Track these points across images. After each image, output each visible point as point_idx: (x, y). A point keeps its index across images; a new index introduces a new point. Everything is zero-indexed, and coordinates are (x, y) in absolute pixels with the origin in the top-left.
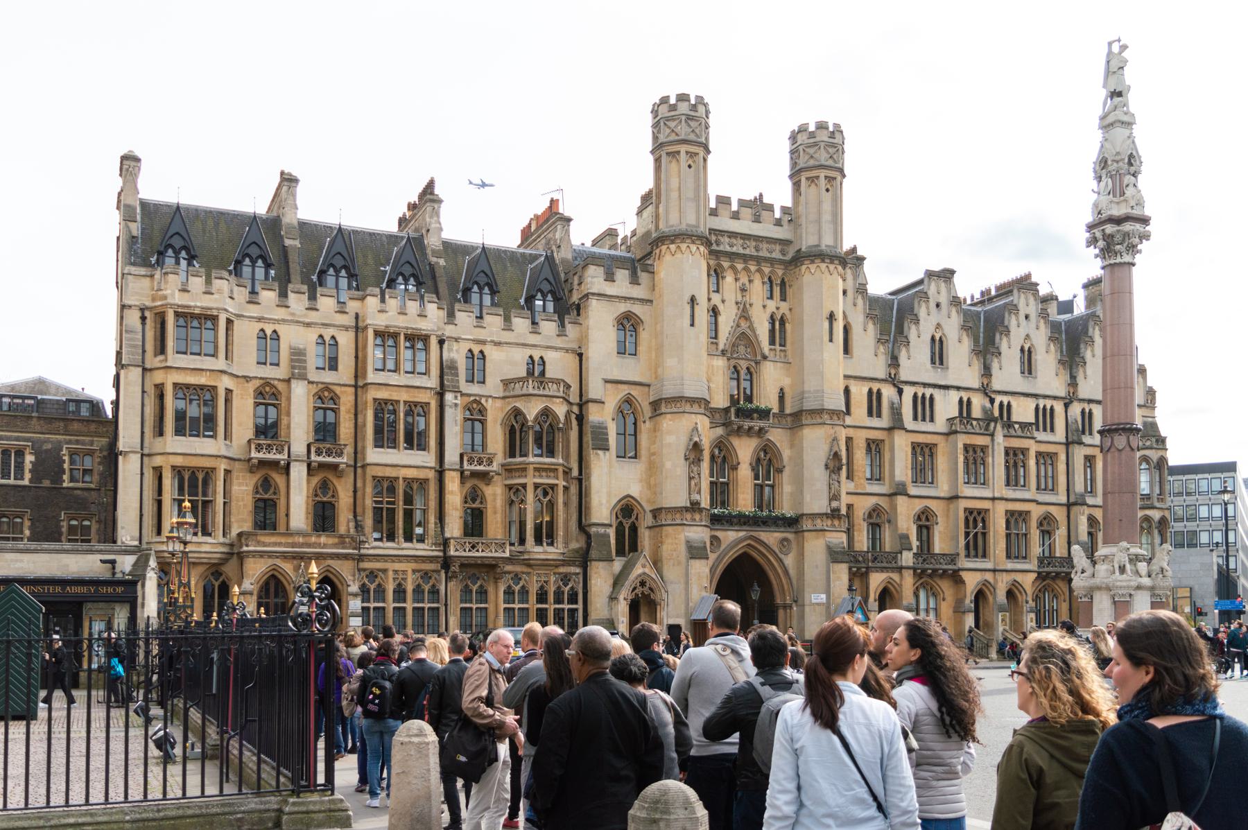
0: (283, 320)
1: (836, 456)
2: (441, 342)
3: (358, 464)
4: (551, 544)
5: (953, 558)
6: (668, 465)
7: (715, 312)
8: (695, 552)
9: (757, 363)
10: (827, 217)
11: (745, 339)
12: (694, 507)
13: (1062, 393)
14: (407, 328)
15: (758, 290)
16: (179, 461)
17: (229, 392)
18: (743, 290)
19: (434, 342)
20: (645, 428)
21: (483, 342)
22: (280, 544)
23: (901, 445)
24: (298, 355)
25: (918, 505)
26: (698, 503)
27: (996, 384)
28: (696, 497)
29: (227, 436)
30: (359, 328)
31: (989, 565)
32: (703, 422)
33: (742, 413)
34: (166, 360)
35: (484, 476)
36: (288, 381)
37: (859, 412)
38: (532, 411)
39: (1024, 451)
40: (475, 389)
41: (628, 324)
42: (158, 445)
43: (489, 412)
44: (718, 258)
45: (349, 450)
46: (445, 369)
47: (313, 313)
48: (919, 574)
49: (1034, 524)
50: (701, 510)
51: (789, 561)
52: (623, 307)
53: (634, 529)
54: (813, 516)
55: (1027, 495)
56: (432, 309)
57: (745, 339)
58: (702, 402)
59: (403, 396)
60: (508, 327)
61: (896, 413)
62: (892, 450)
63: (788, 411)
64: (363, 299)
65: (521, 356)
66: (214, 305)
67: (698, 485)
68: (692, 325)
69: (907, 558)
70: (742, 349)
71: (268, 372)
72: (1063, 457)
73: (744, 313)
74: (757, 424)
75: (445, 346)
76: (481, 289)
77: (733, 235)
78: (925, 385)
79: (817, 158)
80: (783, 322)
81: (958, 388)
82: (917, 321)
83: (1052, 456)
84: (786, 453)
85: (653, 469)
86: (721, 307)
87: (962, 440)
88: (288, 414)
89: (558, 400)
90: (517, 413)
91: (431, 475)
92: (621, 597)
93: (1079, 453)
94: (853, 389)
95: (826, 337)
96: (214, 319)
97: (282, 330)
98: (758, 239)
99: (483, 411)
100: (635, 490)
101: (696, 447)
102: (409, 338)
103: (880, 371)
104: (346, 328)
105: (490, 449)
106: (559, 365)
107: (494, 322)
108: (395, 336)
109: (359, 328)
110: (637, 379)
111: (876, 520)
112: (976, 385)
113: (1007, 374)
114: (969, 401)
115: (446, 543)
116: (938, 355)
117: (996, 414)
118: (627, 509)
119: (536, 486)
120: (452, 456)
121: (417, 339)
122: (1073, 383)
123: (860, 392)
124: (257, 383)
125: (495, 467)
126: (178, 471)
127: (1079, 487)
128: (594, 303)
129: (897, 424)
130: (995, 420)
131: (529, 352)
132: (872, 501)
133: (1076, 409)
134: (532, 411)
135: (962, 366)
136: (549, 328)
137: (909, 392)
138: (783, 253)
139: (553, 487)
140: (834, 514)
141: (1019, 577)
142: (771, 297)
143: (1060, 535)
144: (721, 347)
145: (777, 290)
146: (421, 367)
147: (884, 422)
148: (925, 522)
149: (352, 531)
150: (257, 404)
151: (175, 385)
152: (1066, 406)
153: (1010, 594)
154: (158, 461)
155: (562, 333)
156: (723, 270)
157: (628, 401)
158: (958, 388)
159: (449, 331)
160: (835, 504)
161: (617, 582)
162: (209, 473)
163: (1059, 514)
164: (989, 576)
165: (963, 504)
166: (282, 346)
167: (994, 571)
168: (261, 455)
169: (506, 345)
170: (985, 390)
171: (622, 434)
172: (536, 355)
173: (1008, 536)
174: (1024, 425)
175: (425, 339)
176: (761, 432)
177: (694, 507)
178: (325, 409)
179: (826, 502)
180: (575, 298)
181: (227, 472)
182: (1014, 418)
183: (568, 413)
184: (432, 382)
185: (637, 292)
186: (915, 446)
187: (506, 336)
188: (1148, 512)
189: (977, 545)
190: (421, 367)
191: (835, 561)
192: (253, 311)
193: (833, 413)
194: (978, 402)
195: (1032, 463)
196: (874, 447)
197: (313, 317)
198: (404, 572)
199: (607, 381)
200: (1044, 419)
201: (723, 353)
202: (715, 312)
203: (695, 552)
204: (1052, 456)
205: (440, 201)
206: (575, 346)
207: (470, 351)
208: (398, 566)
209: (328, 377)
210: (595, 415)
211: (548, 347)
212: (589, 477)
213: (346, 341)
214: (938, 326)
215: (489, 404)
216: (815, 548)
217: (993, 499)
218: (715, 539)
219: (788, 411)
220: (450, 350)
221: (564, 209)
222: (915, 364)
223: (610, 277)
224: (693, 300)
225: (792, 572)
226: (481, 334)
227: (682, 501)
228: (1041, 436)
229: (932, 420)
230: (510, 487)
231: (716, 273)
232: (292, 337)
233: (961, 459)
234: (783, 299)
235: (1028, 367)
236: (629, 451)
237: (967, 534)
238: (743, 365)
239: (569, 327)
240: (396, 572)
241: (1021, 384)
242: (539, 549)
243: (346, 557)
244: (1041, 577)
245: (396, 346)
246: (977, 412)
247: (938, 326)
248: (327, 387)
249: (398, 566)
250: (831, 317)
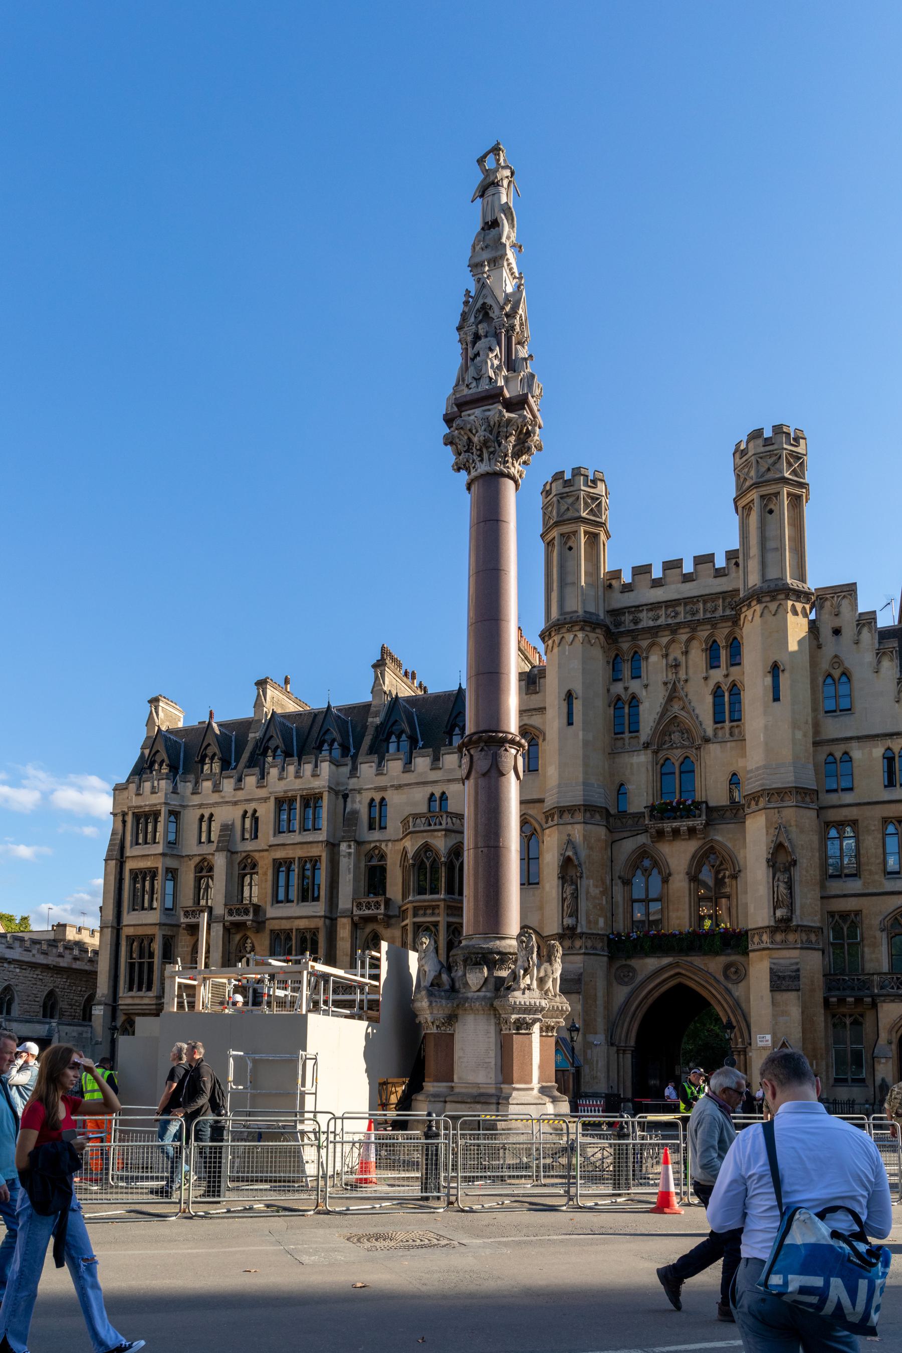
0: (216, 803)
9: (698, 748)
14: (302, 789)
21: (384, 789)
40: (376, 835)
43: (389, 856)
44: (634, 639)
59: (298, 853)
68: (570, 723)
70: (676, 737)
73: (673, 694)
74: (683, 825)
75: (349, 800)
86: (642, 694)
89: (440, 834)
97: (216, 811)
99: (383, 857)
159: (353, 783)
187: (409, 778)
192: (196, 800)
197: (240, 795)
201: (647, 746)
211: (449, 781)
220: (353, 802)
226: (382, 781)
232: (227, 815)
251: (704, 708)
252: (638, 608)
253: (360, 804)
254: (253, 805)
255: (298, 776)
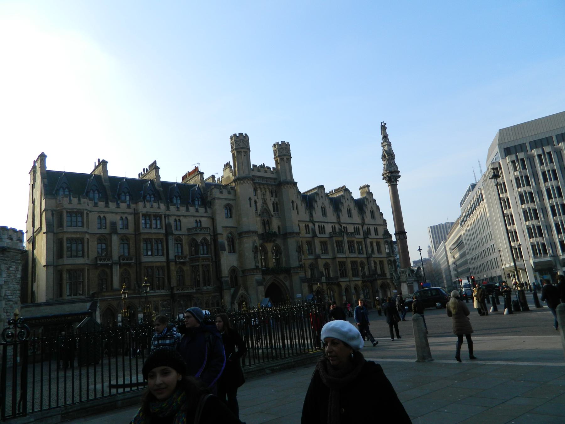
1: (299, 247)
2: (165, 217)
3: (139, 263)
4: (209, 285)
5: (336, 278)
6: (247, 254)
7: (256, 202)
8: (259, 283)
9: (270, 218)
10: (288, 170)
11: (265, 210)
12: (257, 267)
13: (360, 222)
15: (268, 194)
16: (69, 267)
17: (88, 239)
18: (264, 194)
19: (163, 216)
20: (237, 242)
21: (179, 216)
22: (111, 296)
23: (317, 241)
24: (114, 225)
25: (324, 262)
26: (258, 266)
27: (342, 221)
28: (257, 264)
29: (88, 257)
30: (136, 214)
31: (348, 279)
32: (256, 239)
33: (267, 236)
34: (63, 229)
35: (184, 263)
36: (110, 234)
37: (303, 231)
38: (199, 239)
39: (353, 242)
41: (229, 208)
42: (60, 262)
45: (134, 258)
46: (168, 226)
47: (118, 209)
48: (328, 284)
49: (359, 264)
50: (259, 269)
51: (287, 283)
52: (226, 202)
53: (236, 278)
54: (294, 268)
55: (355, 256)
56: (162, 206)
57: (265, 210)
58: (255, 232)
60: (188, 210)
61: (314, 231)
62: (314, 244)
63: (281, 233)
64: (136, 203)
65: (193, 220)
66: (81, 208)
67: (258, 260)
68: (251, 206)
69: (324, 279)
71: (102, 231)
72: (363, 243)
73: (265, 202)
76: (176, 198)
77: (259, 177)
78: (322, 222)
79: (283, 152)
80: (277, 204)
81: (331, 223)
82: (316, 201)
83: (361, 242)
84: (282, 248)
85: (241, 257)
86: (257, 200)
87: (335, 239)
88: (111, 246)
90: (194, 240)
91: (165, 264)
92: (235, 302)
93: (368, 241)
94: (300, 225)
95: (292, 209)
96: (82, 214)
97: (107, 216)
98: (266, 178)
99: (181, 240)
100: (235, 264)
101: (256, 247)
102: (154, 216)
103: (308, 220)
104: (131, 214)
105: (185, 253)
106: (206, 222)
107: (183, 209)
108: (150, 216)
109: (136, 214)
110: (233, 226)
111: (313, 267)
112: (336, 221)
113: (344, 218)
114: (335, 227)
115: (172, 289)
116: (324, 213)
117: (343, 230)
118: (233, 270)
119: (203, 265)
120: (172, 256)
121: (157, 216)
122: (363, 219)
123: (302, 225)
124: (98, 235)
125: (187, 259)
126: (69, 271)
127: (370, 252)
128: (217, 201)
129: (315, 235)
130: (344, 232)
131: (195, 218)
132: (310, 261)
133: (365, 227)
134: (199, 239)
135: (331, 216)
136: (202, 210)
137: (317, 225)
138: (275, 182)
139: (208, 265)
140: (301, 267)
141: (356, 282)
142: (272, 196)
143: (366, 267)
144: (259, 213)
145: (274, 194)
146: (159, 226)
147: (310, 235)
148: (326, 266)
149: (137, 288)
150: (98, 243)
151: (67, 238)
152: (362, 226)
153: (355, 288)
154: (60, 268)
155: (206, 211)
156: (257, 188)
157: (231, 233)
158: (331, 223)
159: (168, 213)
160: (301, 263)
161: (233, 297)
162: (82, 270)
163: (365, 261)
164: (348, 283)
165: (338, 260)
166: (107, 221)
167: (349, 281)
168: (101, 262)
169: (188, 218)
170: (339, 222)
171: (229, 245)
172: (198, 219)
173: (352, 269)
174: (351, 233)
175: (160, 216)
176: (274, 241)
177: (257, 267)
178: (124, 243)
179: (298, 263)
180: (209, 199)
181: (88, 269)
182: (348, 231)
183: (211, 239)
184: (163, 231)
185: (230, 197)
186: (321, 242)
187: (187, 214)
188: (390, 258)
189: (344, 274)
190: (159, 226)
191: (304, 282)
192: (96, 209)
193: (298, 233)
194: (337, 227)
195: (356, 245)
196: (309, 243)
198: (158, 301)
199: (223, 227)
200: (357, 230)
201: (259, 215)
202: (256, 202)
203: (259, 283)
204: (361, 242)
205: (159, 168)
206: (210, 216)
207: (175, 219)
208: (155, 299)
209: (125, 231)
210: (220, 240)
212: (219, 261)
213: (131, 218)
214: (323, 203)
215: (183, 238)
216: (296, 279)
217: (346, 258)
218: (264, 278)
219: (281, 233)
220: (168, 219)
221: (201, 170)
222: (318, 215)
223: (221, 192)
224: (250, 199)
225: (289, 288)
227: (253, 266)
228: (357, 236)
229: (325, 233)
230: (192, 266)
231: (255, 190)
232: (110, 218)
233: (335, 246)
234: (276, 197)
235: (350, 215)
236: (233, 250)
237: (340, 270)
238: (266, 219)
239: (208, 210)
240: (154, 301)
241: (349, 220)
242: (205, 288)
243: (136, 298)
244: (363, 282)
245: (150, 219)
246: (337, 230)
247: (323, 203)
248: (125, 235)
249: (155, 299)
250: (293, 202)
251: (271, 207)
252: (255, 176)
253: (172, 220)
254: (126, 215)
255: (152, 207)
